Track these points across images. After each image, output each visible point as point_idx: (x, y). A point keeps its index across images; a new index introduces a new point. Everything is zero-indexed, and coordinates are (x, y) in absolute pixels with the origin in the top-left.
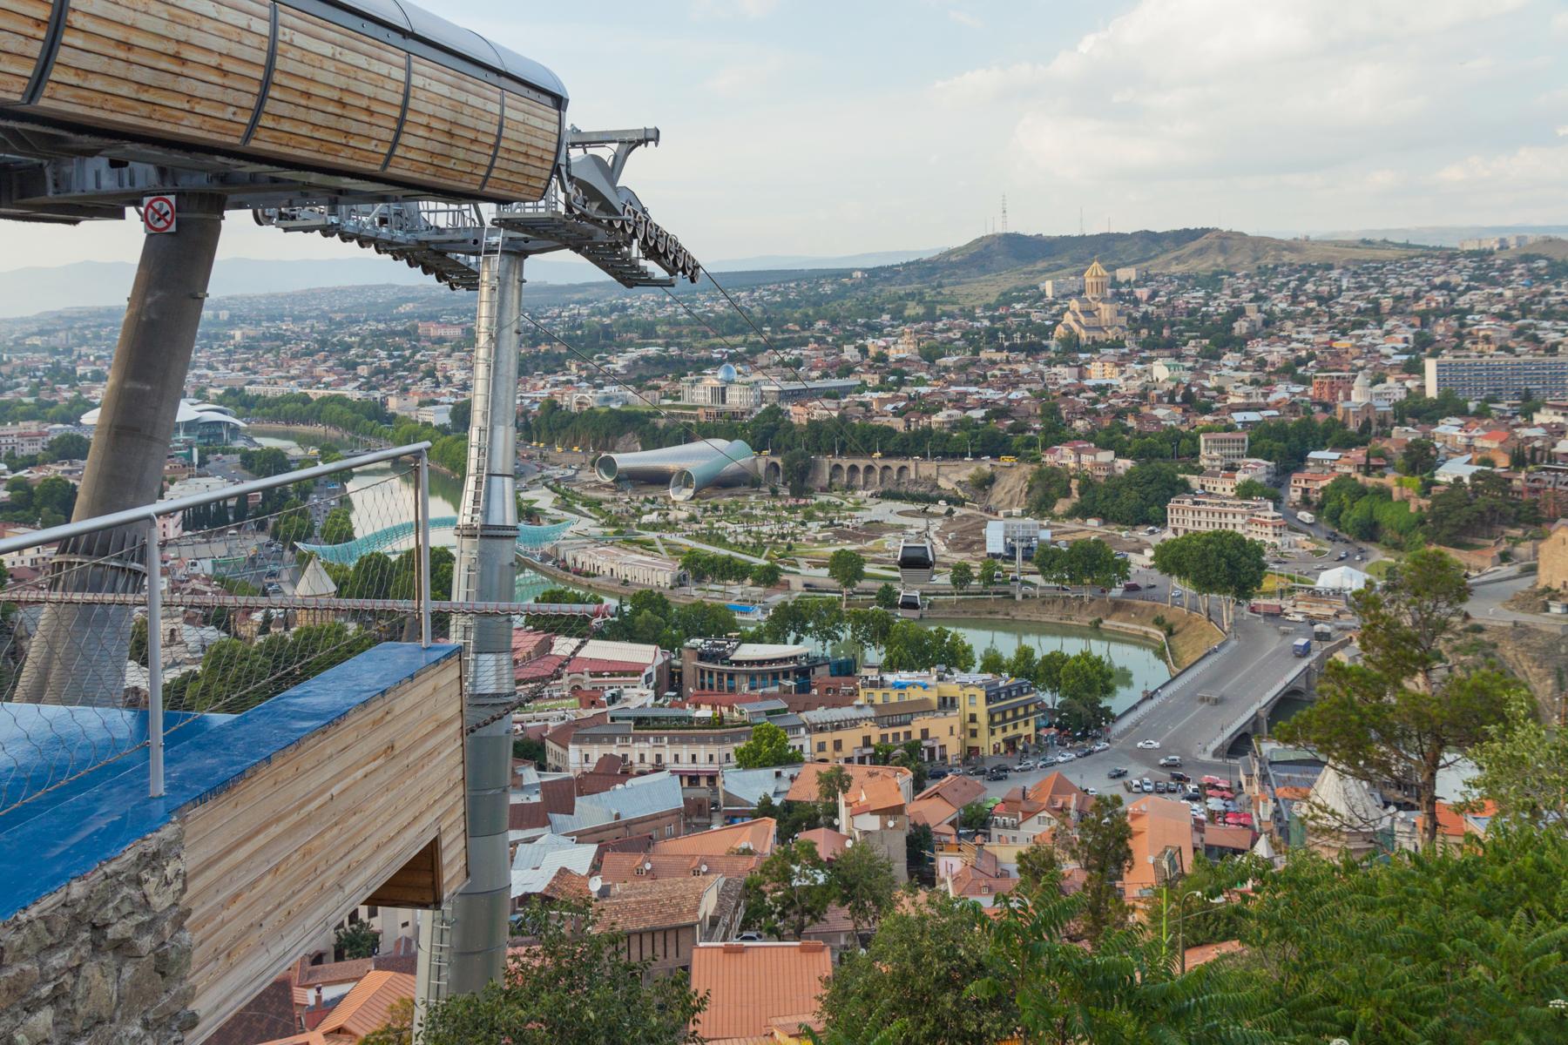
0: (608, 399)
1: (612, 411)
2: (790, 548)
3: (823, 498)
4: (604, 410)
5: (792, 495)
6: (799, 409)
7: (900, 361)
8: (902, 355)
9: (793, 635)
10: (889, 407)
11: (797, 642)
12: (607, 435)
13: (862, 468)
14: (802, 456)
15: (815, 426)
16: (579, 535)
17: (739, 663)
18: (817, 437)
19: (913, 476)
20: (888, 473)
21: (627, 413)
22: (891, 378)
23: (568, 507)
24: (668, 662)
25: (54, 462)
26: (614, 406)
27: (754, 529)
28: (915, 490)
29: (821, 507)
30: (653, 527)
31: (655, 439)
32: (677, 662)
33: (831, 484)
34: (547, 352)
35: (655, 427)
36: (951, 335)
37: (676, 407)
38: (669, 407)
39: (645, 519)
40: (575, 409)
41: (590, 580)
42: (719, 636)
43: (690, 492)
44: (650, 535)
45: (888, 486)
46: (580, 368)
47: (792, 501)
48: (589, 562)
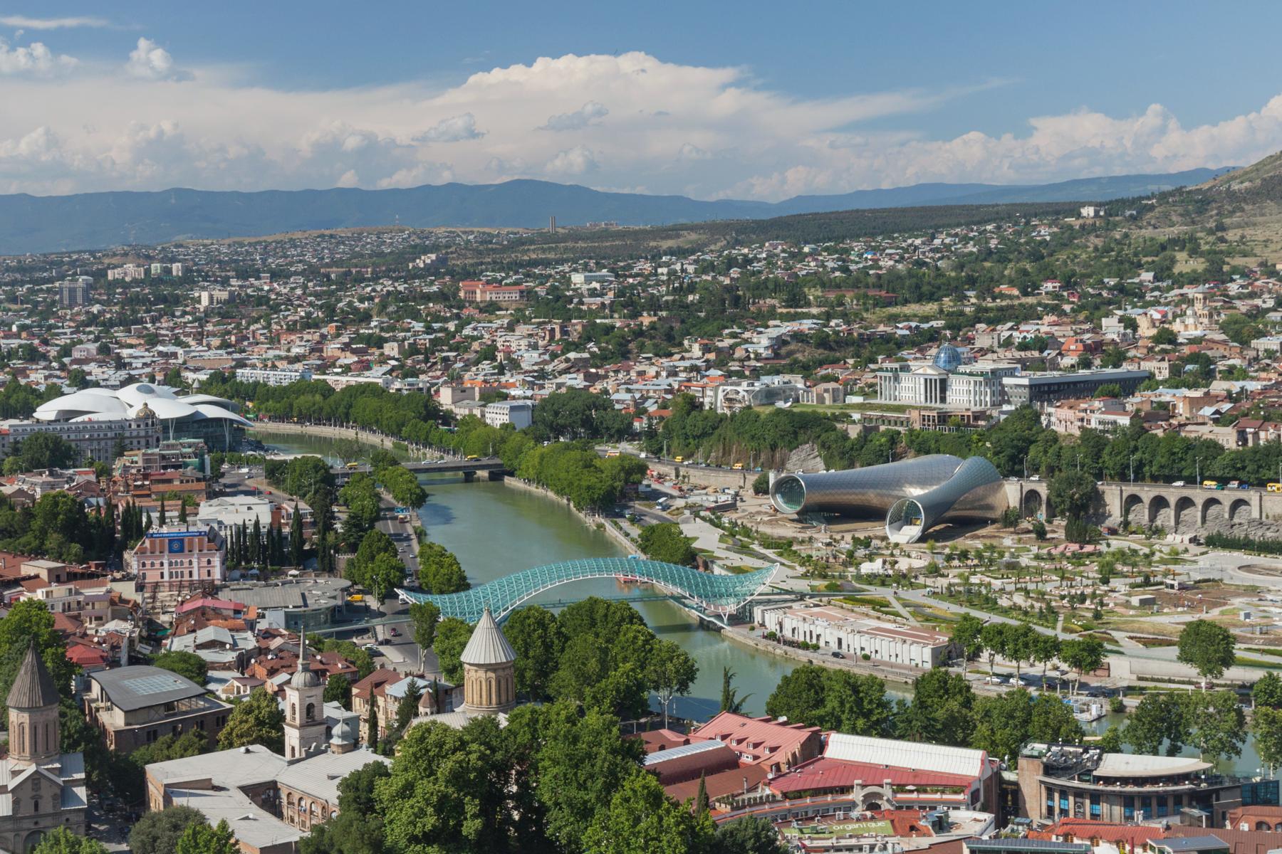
0: (770, 395)
1: (780, 412)
2: (1098, 616)
3: (1116, 543)
4: (768, 410)
5: (1070, 538)
6: (1065, 413)
7: (1192, 341)
8: (1198, 333)
9: (1166, 742)
10: (1208, 411)
11: (1173, 752)
12: (773, 448)
13: (1172, 501)
14: (1080, 482)
15: (1094, 441)
17: (1109, 780)
18: (1097, 456)
19: (1255, 514)
20: (1213, 510)
21: (802, 414)
22: (1189, 367)
23: (744, 549)
24: (997, 775)
25: (28, 471)
26: (780, 404)
27: (1031, 587)
28: (1256, 535)
29: (1122, 556)
30: (883, 581)
31: (848, 454)
32: (1008, 776)
33: (1126, 524)
34: (653, 326)
35: (845, 437)
36: (1258, 302)
38: (860, 407)
39: (866, 568)
40: (722, 409)
42: (1068, 742)
43: (914, 531)
44: (876, 592)
45: (1212, 528)
46: (706, 349)
47: (1074, 547)
48: (804, 627)
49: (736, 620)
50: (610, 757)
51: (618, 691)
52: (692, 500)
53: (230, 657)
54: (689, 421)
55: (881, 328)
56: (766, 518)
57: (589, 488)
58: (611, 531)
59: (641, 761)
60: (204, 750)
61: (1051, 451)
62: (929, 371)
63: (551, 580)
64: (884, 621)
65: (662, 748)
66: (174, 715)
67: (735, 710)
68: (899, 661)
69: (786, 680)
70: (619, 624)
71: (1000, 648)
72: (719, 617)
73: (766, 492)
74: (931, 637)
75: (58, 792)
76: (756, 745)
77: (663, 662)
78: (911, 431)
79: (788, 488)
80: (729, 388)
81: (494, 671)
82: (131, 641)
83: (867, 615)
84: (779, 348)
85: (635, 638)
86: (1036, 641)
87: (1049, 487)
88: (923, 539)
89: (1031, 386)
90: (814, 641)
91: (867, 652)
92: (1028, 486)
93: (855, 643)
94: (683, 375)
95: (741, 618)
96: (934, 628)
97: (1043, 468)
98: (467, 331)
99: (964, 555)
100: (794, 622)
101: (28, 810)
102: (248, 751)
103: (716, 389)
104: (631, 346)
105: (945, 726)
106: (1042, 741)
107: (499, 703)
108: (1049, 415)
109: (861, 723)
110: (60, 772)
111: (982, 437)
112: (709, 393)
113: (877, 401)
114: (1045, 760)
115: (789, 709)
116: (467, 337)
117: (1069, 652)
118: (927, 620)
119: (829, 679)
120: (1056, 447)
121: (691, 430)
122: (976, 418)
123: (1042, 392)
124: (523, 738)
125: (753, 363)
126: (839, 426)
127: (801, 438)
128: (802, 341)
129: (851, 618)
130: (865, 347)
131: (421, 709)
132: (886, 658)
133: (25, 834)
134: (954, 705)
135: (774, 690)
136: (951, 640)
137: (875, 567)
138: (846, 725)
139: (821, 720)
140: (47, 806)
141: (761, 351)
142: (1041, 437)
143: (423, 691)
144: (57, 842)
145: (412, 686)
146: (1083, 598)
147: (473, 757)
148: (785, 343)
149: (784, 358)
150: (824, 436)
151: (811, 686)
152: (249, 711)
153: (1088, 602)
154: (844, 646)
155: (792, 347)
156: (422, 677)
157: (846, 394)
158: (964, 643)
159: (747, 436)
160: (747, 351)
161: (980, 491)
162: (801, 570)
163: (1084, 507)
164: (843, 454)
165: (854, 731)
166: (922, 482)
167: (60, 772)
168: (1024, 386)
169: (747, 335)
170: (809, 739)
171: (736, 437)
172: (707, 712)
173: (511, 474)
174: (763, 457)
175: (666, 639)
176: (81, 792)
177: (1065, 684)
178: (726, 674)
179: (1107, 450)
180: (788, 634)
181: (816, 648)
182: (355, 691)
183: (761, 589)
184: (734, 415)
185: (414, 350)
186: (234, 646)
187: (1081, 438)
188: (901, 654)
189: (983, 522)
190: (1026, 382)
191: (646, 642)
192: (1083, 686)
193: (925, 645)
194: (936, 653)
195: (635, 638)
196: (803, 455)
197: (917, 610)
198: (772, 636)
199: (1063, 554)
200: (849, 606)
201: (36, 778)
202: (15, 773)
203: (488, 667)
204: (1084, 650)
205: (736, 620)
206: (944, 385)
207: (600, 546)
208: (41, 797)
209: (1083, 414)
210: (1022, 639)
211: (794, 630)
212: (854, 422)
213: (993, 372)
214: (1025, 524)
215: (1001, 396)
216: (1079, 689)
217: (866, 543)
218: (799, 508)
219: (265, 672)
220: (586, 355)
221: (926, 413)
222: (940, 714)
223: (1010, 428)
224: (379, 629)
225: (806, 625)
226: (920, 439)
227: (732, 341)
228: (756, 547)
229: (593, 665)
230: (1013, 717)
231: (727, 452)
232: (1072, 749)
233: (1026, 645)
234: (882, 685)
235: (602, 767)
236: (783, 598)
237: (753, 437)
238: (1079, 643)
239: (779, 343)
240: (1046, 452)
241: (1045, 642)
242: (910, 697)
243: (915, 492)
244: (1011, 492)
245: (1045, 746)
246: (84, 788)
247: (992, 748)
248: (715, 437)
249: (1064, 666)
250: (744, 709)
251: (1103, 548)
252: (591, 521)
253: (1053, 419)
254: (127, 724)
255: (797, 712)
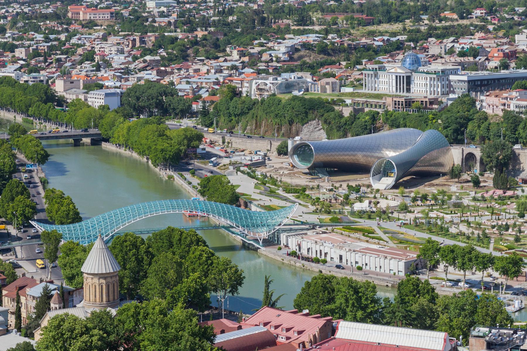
0: (288, 87)
1: (295, 98)
2: (517, 240)
4: (287, 97)
5: (497, 186)
12: (291, 123)
15: (513, 120)
16: (296, 222)
18: (515, 130)
21: (311, 100)
23: (272, 193)
26: (296, 93)
27: (471, 219)
30: (370, 215)
31: (341, 127)
34: (204, 38)
35: (341, 116)
37: (360, 95)
38: (351, 95)
39: (358, 206)
40: (255, 96)
41: (320, 266)
42: (502, 327)
43: (390, 181)
46: (242, 54)
47: (500, 192)
48: (316, 248)
49: (269, 242)
50: (191, 338)
51: (189, 292)
52: (234, 159)
54: (232, 104)
55: (364, 40)
56: (286, 172)
57: (162, 150)
58: (178, 180)
59: (212, 341)
61: (483, 126)
62: (399, 71)
63: (143, 215)
64: (371, 243)
65: (223, 332)
67: (273, 305)
68: (382, 270)
69: (308, 285)
70: (189, 246)
71: (453, 263)
72: (256, 240)
73: (286, 154)
74: (404, 255)
76: (288, 330)
77: (220, 272)
78: (387, 112)
79: (302, 151)
80: (260, 81)
81: (105, 278)
83: (359, 239)
84: (293, 54)
85: (201, 255)
86: (477, 257)
87: (482, 151)
88: (396, 186)
89: (469, 82)
90: (323, 257)
91: (360, 265)
92: (468, 149)
93: (351, 258)
94: (226, 72)
95: (271, 241)
96: (406, 248)
97: (477, 138)
98: (74, 40)
99: (424, 198)
100: (309, 244)
103: (250, 82)
104: (190, 51)
105: (418, 315)
106: (484, 325)
107: (108, 301)
108: (482, 101)
109: (359, 314)
111: (436, 116)
112: (246, 85)
113: (363, 91)
114: (487, 338)
115: (310, 305)
116: (74, 45)
117: (500, 264)
118: (401, 243)
119: (338, 283)
120: (486, 123)
121: (233, 110)
122: (431, 103)
123: (478, 85)
124: (129, 325)
125: (275, 64)
126: (336, 108)
127: (310, 116)
128: (309, 49)
129: (349, 241)
130: (352, 54)
131: (52, 305)
132: (373, 269)
134: (424, 301)
135: (299, 291)
136: (419, 256)
137: (364, 206)
138: (350, 315)
139: (333, 312)
141: (280, 55)
142: (476, 116)
143: (53, 292)
145: (46, 289)
146: (507, 227)
147: (95, 339)
148: (297, 50)
149: (296, 61)
150: (326, 115)
151: (325, 288)
153: (510, 230)
154: (344, 260)
155: (302, 53)
156: (52, 282)
157: (341, 86)
158: (428, 258)
159: (272, 115)
160: (271, 55)
161: (434, 153)
162: (312, 208)
163: (506, 165)
164: (339, 128)
165: (355, 319)
166: (394, 147)
168: (464, 81)
169: (270, 44)
170: (325, 325)
171: (264, 115)
172: (252, 307)
173: (107, 140)
174: (283, 129)
175: (222, 256)
177: (497, 287)
178: (266, 281)
179: (521, 126)
180: (304, 252)
181: (325, 262)
182: (4, 292)
183: (286, 221)
184: (263, 101)
185: (36, 54)
187: (504, 117)
188: (383, 266)
189: (437, 175)
190: (465, 78)
191: (208, 258)
192: (509, 288)
193: (400, 260)
194: (408, 265)
195: (201, 255)
196: (312, 128)
197: (393, 236)
198: (293, 254)
199: (492, 197)
200: (347, 233)
203: (101, 276)
204: (510, 263)
205: (269, 242)
206: (409, 80)
207: (170, 192)
209: (505, 101)
210: (467, 256)
211: (308, 249)
212: (347, 105)
213: (443, 71)
214: (465, 176)
215: (449, 88)
216: (506, 290)
217: (357, 189)
218: (309, 165)
220: (158, 58)
221: (397, 99)
222: (415, 307)
223: (455, 110)
224: (18, 249)
225: (318, 246)
226: (393, 117)
227: (260, 49)
228: (280, 192)
229: (172, 274)
230: (464, 310)
231: (258, 126)
232: (505, 331)
233: (470, 260)
234: (374, 287)
235: (185, 346)
236: (302, 227)
237: (276, 116)
238: (507, 258)
239: (294, 50)
240: (479, 127)
241: (483, 258)
242: (392, 295)
243: (390, 154)
244: (455, 155)
245: (488, 329)
247: (450, 330)
248: (250, 115)
249: (496, 274)
250: (278, 305)
251: (519, 192)
252: (164, 174)
253: (484, 104)
255: (316, 306)
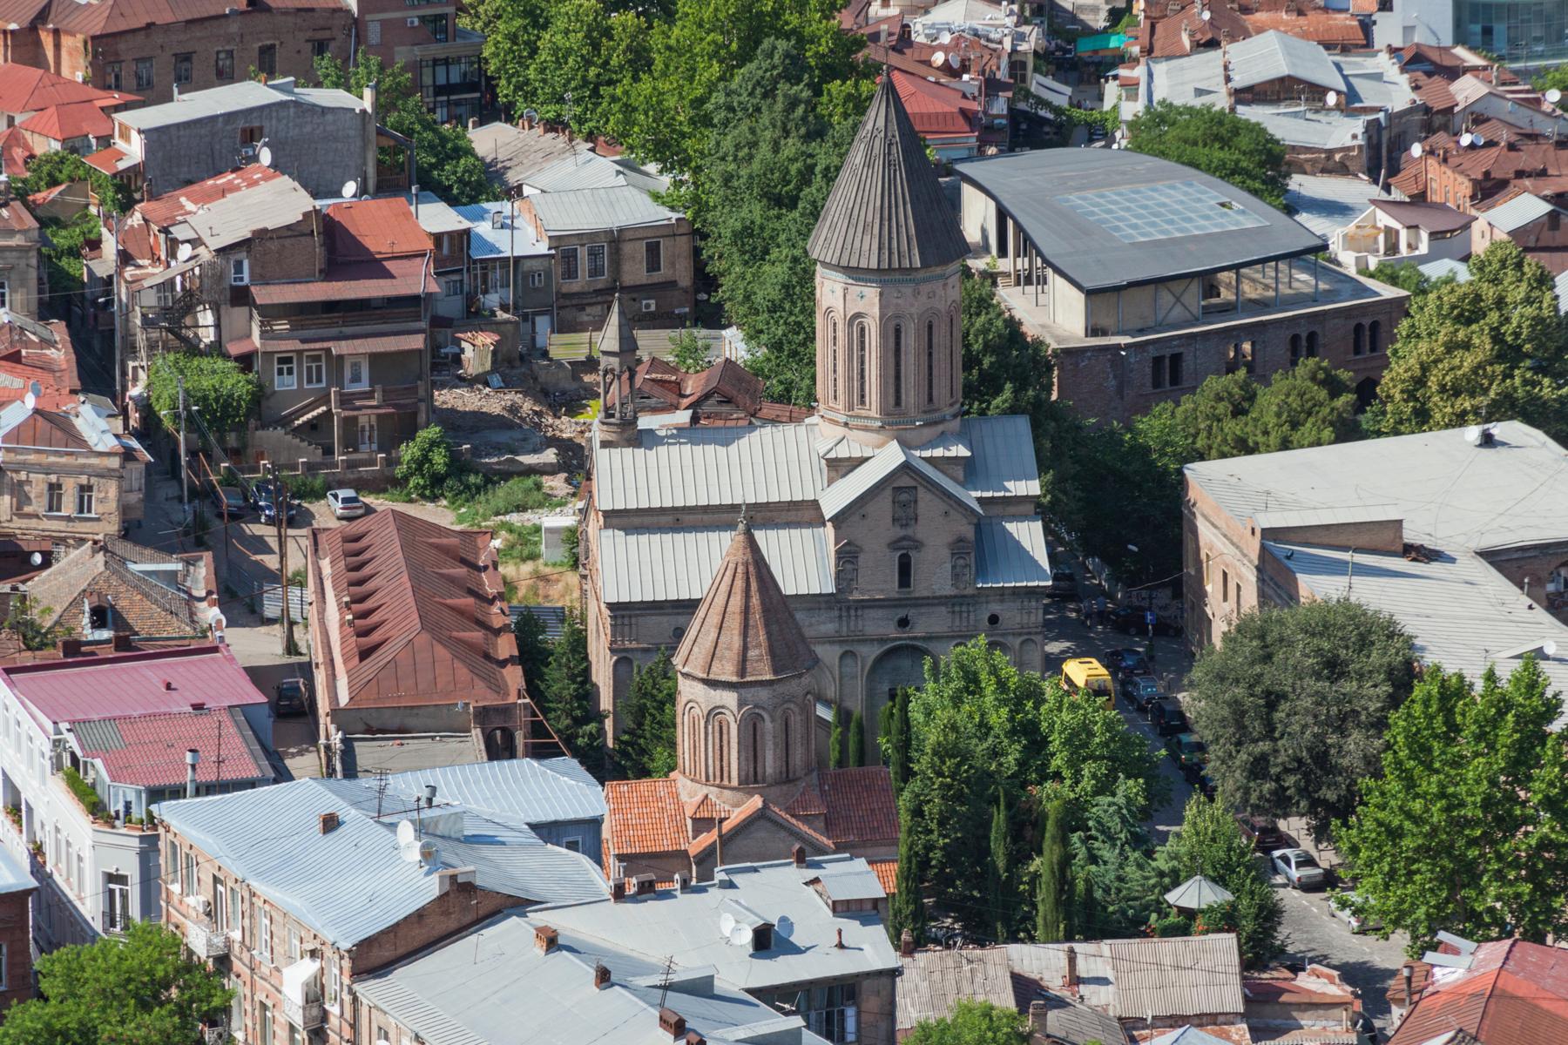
53: (1345, 133)
60: (1347, 431)
66: (1227, 309)
75: (969, 532)
82: (1017, 66)
101: (879, 581)
102: (1488, 441)
110: (970, 471)
133: (871, 652)
140: (934, 576)
144: (972, 683)
152: (1468, 312)
167: (970, 471)
176: (1030, 536)
186: (1350, 102)
201: (901, 488)
202: (840, 467)
208: (918, 545)
219: (1465, 188)
246: (1037, 527)
254: (1092, 331)
